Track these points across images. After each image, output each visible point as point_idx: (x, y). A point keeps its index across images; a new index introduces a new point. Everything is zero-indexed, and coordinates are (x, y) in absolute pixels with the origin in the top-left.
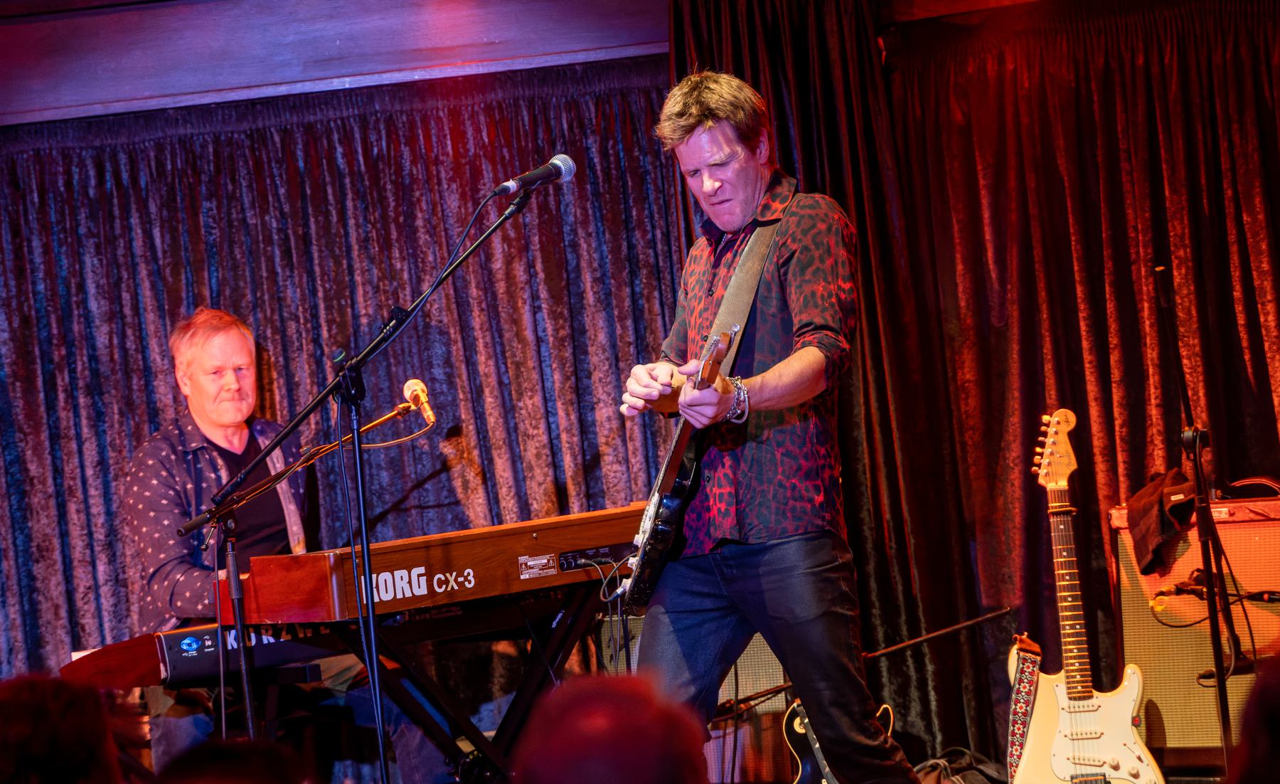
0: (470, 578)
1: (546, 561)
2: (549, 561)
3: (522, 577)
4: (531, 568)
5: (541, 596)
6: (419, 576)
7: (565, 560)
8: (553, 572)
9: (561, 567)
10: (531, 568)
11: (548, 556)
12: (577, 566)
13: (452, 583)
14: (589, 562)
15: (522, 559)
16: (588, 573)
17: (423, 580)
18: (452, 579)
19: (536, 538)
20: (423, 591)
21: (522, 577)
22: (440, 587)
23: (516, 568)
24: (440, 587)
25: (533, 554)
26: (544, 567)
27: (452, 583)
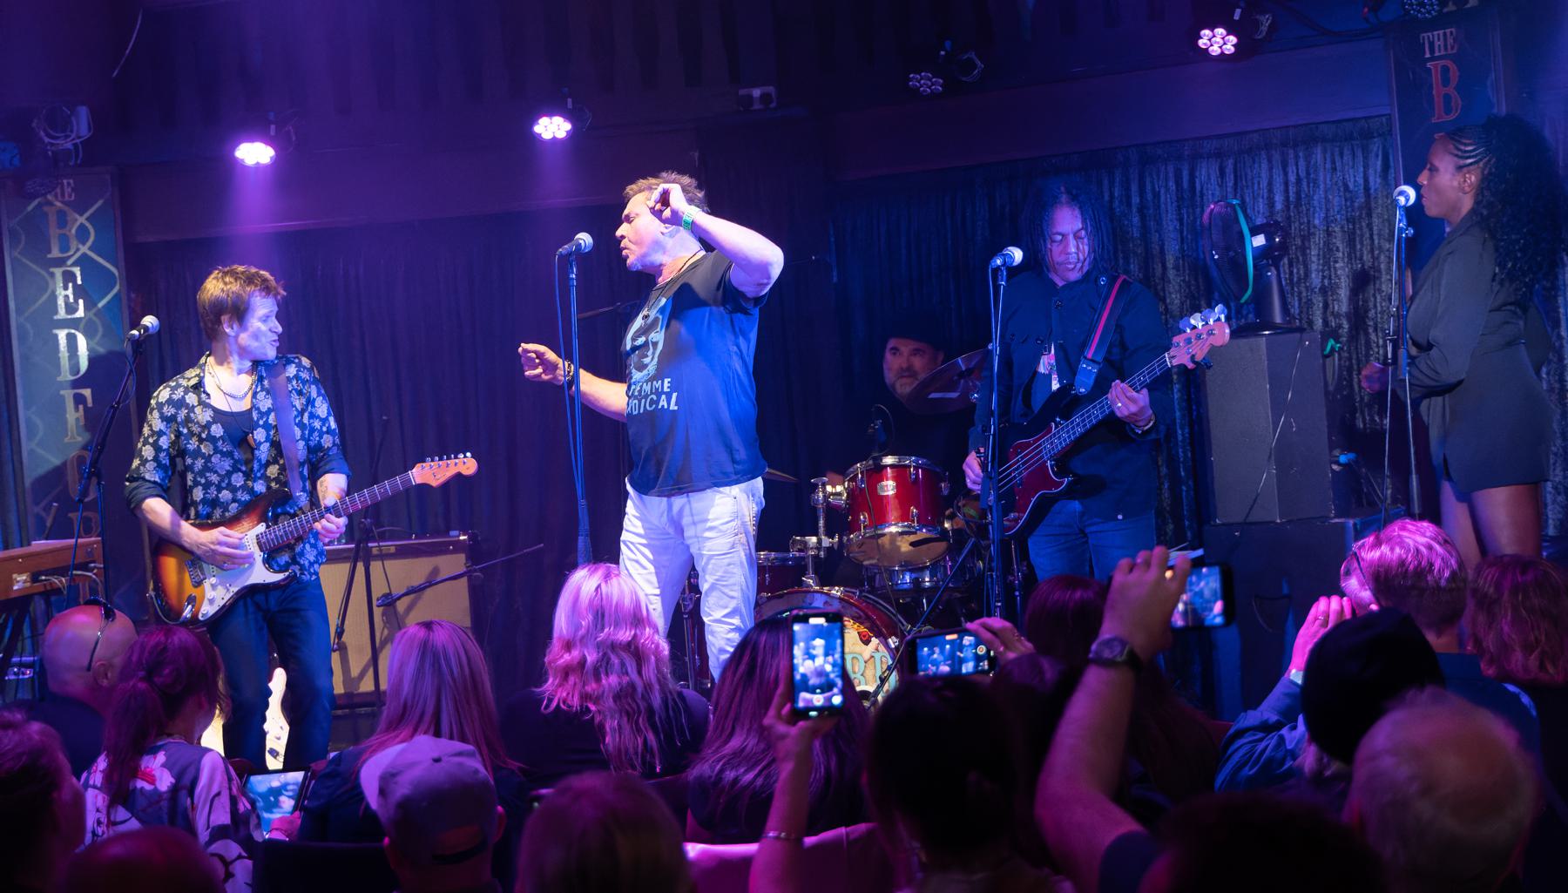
1: (24, 578)
3: (15, 588)
4: (18, 582)
7: (34, 578)
8: (28, 584)
10: (18, 582)
12: (43, 580)
14: (47, 578)
15: (15, 576)
16: (45, 585)
19: (21, 563)
21: (15, 588)
23: (11, 582)
25: (20, 573)
26: (25, 582)
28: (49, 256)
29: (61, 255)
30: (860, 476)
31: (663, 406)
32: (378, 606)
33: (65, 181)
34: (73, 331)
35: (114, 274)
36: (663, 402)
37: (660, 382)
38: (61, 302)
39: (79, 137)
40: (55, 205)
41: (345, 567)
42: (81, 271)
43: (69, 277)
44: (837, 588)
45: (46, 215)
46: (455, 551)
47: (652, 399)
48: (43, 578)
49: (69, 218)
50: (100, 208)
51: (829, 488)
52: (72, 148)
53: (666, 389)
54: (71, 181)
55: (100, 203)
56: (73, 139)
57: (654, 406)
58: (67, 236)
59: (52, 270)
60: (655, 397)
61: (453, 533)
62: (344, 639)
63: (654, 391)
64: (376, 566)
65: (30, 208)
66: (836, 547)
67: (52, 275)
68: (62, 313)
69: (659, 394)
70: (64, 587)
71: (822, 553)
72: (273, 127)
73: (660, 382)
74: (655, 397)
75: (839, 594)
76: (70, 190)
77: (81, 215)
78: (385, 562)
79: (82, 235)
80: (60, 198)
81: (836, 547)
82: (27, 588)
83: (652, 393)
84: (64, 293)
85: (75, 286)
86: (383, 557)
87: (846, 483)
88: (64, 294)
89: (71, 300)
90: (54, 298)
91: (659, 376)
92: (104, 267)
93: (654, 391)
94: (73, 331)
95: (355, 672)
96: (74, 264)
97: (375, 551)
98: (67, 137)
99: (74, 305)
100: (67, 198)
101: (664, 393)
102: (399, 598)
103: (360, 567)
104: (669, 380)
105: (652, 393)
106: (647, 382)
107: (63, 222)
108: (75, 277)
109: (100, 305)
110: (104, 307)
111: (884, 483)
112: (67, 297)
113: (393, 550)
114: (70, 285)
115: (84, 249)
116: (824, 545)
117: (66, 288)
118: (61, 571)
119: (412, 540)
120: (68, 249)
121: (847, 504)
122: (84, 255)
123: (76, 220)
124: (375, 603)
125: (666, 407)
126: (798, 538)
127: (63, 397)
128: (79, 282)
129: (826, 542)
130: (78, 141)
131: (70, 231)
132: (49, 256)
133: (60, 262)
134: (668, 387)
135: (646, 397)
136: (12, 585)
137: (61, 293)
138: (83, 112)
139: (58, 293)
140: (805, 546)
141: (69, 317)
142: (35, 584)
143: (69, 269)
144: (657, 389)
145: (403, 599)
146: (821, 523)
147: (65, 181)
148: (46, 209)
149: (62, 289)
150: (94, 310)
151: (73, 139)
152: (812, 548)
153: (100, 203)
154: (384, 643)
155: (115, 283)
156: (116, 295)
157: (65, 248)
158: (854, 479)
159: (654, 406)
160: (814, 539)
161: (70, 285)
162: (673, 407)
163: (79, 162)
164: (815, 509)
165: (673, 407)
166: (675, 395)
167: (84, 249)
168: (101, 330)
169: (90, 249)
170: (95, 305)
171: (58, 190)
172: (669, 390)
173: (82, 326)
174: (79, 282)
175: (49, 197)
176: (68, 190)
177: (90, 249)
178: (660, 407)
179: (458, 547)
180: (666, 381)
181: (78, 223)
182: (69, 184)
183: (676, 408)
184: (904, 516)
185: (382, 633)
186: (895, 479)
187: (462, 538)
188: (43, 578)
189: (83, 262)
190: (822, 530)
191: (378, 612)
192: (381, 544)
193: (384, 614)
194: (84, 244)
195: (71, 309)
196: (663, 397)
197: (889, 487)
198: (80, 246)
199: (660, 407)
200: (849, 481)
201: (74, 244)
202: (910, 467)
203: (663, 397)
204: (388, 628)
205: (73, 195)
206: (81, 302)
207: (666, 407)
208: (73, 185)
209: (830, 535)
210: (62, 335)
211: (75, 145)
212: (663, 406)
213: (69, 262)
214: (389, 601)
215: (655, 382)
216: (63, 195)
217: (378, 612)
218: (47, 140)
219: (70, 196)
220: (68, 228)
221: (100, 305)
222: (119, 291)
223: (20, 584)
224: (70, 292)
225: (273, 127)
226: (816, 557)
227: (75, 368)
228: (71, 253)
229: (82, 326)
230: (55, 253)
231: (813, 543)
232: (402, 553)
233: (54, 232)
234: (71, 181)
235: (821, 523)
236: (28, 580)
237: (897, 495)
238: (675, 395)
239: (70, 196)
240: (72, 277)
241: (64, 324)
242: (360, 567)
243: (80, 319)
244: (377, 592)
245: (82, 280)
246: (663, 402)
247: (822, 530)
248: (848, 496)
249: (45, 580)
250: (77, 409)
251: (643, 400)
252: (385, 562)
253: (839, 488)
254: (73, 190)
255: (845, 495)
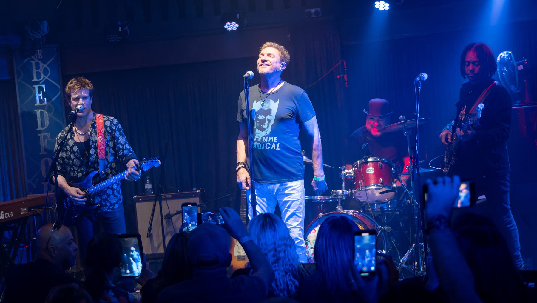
0: (12, 214)
1: (25, 209)
2: (26, 209)
3: (22, 214)
4: (23, 211)
5: (25, 219)
6: (2, 213)
7: (29, 210)
9: (29, 211)
11: (26, 208)
13: (9, 216)
14: (34, 209)
15: (21, 209)
17: (3, 214)
18: (8, 214)
20: (3, 218)
21: (22, 214)
22: (6, 216)
23: (20, 211)
24: (6, 216)
25: (23, 208)
26: (25, 211)
27: (9, 216)
28: (33, 81)
29: (37, 80)
30: (359, 166)
31: (273, 148)
32: (165, 219)
33: (39, 51)
34: (42, 110)
35: (58, 87)
36: (273, 146)
37: (272, 138)
38: (37, 99)
39: (44, 33)
40: (35, 60)
41: (151, 204)
42: (45, 86)
43: (40, 89)
44: (350, 211)
45: (32, 63)
46: (195, 196)
47: (268, 144)
48: (33, 209)
49: (40, 65)
50: (53, 61)
51: (346, 171)
52: (41, 37)
53: (275, 141)
54: (41, 50)
55: (53, 59)
56: (41, 34)
57: (269, 147)
58: (40, 72)
59: (34, 86)
60: (270, 144)
61: (194, 189)
62: (151, 232)
63: (269, 141)
64: (164, 203)
65: (25, 61)
66: (350, 195)
67: (34, 88)
68: (38, 103)
69: (272, 143)
70: (41, 213)
71: (344, 197)
72: (120, 28)
73: (272, 138)
74: (270, 144)
75: (351, 214)
76: (40, 54)
77: (45, 64)
78: (168, 201)
79: (45, 72)
80: (36, 58)
81: (350, 195)
82: (26, 214)
83: (268, 142)
84: (38, 95)
85: (43, 93)
86: (166, 199)
87: (353, 169)
88: (39, 96)
89: (42, 98)
90: (35, 97)
91: (272, 134)
92: (55, 85)
93: (269, 141)
94: (42, 110)
95: (156, 245)
96: (42, 84)
97: (163, 197)
98: (39, 33)
99: (43, 100)
100: (39, 58)
101: (275, 143)
102: (173, 216)
103: (158, 203)
104: (276, 137)
105: (268, 142)
106: (266, 136)
107: (38, 67)
108: (43, 89)
109: (53, 100)
110: (54, 100)
111: (369, 169)
112: (40, 97)
113: (170, 196)
114: (41, 92)
115: (46, 78)
116: (344, 194)
117: (39, 93)
118: (39, 207)
119: (178, 192)
120: (40, 78)
121: (354, 177)
122: (46, 80)
123: (43, 66)
124: (164, 217)
125: (275, 148)
126: (334, 191)
127: (39, 136)
128: (45, 91)
129: (346, 192)
130: (43, 34)
131: (41, 70)
132: (33, 81)
133: (37, 83)
134: (276, 141)
135: (265, 143)
136: (21, 213)
137: (37, 95)
138: (45, 23)
139: (36, 95)
140: (337, 193)
141: (41, 104)
142: (29, 212)
143: (40, 85)
144: (271, 141)
145: (174, 216)
146: (343, 185)
147: (39, 51)
148: (31, 62)
149: (38, 94)
150: (51, 102)
151: (41, 34)
152: (340, 195)
153: (53, 59)
154: (167, 233)
155: (59, 91)
156: (59, 96)
157: (39, 77)
158: (357, 167)
159: (269, 147)
160: (341, 191)
161: (41, 92)
162: (278, 149)
163: (44, 43)
164: (341, 179)
165: (278, 149)
166: (279, 144)
167: (46, 78)
168: (53, 109)
169: (49, 77)
170: (51, 100)
171: (36, 54)
172: (276, 142)
173: (46, 107)
174: (45, 91)
175: (32, 57)
176: (39, 54)
177: (49, 77)
178: (272, 148)
179: (197, 195)
180: (275, 138)
181: (44, 67)
182: (40, 51)
183: (279, 149)
184: (377, 183)
185: (166, 232)
186: (373, 167)
187: (198, 191)
188: (33, 209)
189: (46, 83)
190: (344, 188)
191: (165, 221)
192: (166, 194)
193: (167, 222)
194: (46, 75)
195: (41, 101)
196: (274, 144)
197: (370, 170)
198: (45, 76)
199: (272, 148)
200: (354, 168)
201: (42, 76)
202: (379, 162)
203: (274, 144)
204: (169, 227)
205: (42, 56)
206: (45, 99)
207: (275, 148)
208: (41, 52)
209: (347, 189)
210: (38, 112)
211: (42, 36)
212: (273, 148)
213: (41, 83)
214: (169, 217)
215: (270, 138)
216: (38, 57)
217: (165, 221)
218: (31, 34)
219: (40, 57)
220: (40, 70)
221: (53, 100)
222: (61, 94)
223: (23, 212)
224: (41, 95)
225: (120, 28)
226: (341, 198)
227: (43, 125)
228: (41, 79)
229: (46, 107)
230: (35, 79)
231: (340, 193)
232: (174, 197)
233: (35, 71)
234: (41, 50)
235: (343, 185)
236: (27, 210)
237: (375, 173)
238: (279, 144)
239: (40, 57)
240: (40, 89)
241: (39, 107)
242: (158, 203)
243: (45, 106)
244: (164, 214)
245: (46, 90)
246: (273, 146)
247: (344, 188)
248: (354, 175)
249: (33, 210)
250: (44, 141)
251: (264, 144)
252: (167, 201)
253: (351, 171)
254: (41, 55)
255: (353, 173)
